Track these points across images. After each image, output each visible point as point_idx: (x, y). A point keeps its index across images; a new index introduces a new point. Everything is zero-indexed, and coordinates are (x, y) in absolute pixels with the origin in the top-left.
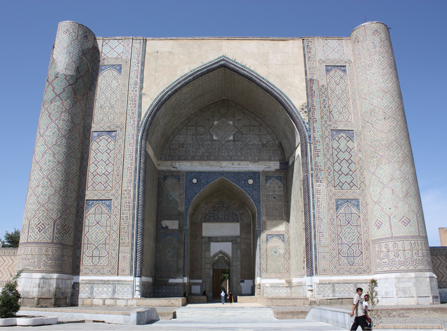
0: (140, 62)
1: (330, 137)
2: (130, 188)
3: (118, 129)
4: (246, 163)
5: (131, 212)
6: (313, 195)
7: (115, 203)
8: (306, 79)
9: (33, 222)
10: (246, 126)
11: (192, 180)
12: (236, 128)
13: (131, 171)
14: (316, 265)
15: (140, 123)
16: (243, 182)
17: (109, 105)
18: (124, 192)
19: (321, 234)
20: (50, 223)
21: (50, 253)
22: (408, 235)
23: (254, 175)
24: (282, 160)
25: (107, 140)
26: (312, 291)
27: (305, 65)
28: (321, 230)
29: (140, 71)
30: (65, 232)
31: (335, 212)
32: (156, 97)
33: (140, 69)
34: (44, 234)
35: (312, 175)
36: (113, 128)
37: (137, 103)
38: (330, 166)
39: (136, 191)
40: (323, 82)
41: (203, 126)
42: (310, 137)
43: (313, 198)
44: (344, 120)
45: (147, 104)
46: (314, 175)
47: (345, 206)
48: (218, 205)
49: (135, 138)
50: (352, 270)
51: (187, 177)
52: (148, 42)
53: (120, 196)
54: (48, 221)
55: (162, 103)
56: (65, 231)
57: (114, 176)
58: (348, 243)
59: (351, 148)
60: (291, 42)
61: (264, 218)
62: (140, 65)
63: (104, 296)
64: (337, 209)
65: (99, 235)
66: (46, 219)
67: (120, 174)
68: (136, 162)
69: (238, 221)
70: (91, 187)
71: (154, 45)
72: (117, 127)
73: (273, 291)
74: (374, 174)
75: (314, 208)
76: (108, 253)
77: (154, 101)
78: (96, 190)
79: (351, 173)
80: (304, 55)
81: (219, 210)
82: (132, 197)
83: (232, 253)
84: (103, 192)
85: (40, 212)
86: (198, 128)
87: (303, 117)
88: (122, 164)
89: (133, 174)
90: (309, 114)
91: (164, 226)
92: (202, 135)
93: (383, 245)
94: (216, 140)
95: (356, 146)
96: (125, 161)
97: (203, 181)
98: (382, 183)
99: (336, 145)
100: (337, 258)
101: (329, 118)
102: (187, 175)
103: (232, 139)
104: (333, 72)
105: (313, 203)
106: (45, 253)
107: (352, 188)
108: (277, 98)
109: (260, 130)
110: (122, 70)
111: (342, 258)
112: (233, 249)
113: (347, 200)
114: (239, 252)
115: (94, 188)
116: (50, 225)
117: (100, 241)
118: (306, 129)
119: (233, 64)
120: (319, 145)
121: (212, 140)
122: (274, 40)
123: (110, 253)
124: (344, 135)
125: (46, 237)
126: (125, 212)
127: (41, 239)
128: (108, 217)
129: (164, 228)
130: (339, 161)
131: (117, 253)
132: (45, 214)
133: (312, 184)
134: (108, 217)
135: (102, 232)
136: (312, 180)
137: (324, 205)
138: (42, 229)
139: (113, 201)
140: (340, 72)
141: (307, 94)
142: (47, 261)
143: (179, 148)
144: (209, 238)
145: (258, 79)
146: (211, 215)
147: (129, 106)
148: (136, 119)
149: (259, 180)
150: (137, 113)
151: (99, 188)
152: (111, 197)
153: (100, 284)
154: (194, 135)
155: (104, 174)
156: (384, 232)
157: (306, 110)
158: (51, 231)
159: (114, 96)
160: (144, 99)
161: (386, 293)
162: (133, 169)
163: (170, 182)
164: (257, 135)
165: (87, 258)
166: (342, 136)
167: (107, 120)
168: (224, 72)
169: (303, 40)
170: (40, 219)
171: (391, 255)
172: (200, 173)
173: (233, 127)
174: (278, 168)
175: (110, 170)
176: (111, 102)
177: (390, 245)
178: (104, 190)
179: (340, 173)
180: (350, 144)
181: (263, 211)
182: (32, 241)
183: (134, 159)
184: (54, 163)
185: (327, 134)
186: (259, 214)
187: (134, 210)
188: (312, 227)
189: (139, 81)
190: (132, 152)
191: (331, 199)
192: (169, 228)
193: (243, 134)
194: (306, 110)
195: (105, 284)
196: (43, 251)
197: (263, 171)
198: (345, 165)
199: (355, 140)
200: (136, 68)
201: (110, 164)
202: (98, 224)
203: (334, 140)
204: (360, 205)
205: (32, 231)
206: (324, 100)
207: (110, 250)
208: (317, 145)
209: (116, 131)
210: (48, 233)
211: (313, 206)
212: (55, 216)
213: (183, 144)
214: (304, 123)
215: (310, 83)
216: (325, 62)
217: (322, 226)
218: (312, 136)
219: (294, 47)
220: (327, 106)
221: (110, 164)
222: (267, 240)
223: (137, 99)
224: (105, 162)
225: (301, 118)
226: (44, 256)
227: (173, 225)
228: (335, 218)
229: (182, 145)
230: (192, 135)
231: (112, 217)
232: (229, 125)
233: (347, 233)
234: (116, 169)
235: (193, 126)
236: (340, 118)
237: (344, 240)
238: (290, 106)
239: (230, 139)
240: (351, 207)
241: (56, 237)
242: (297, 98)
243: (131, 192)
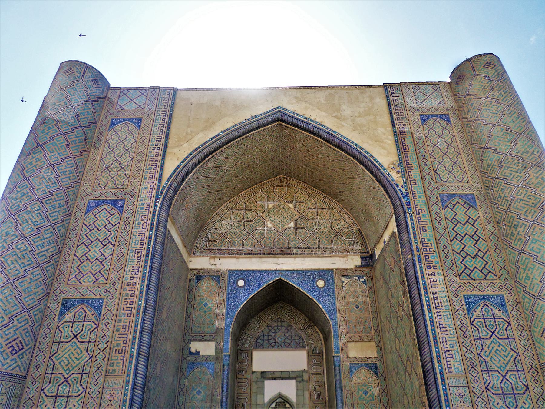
3: (127, 198)
6: (425, 289)
10: (311, 209)
11: (237, 282)
12: (298, 212)
13: (139, 255)
17: (118, 165)
18: (126, 286)
19: (447, 353)
23: (325, 274)
24: (364, 253)
25: (109, 212)
28: (448, 346)
30: (11, 352)
31: (467, 316)
35: (419, 258)
38: (446, 244)
39: (145, 284)
41: (253, 210)
42: (408, 204)
44: (456, 181)
46: (423, 258)
47: (482, 305)
48: (275, 324)
51: (229, 278)
56: (11, 349)
58: (499, 370)
59: (475, 219)
64: (469, 310)
65: (73, 358)
68: (149, 242)
69: (304, 347)
70: (74, 279)
75: (429, 309)
76: (85, 390)
78: (81, 284)
79: (481, 254)
81: (277, 331)
82: (137, 293)
83: (297, 396)
84: (91, 288)
87: (395, 179)
89: (143, 259)
91: (193, 350)
92: (252, 221)
95: (481, 216)
97: (253, 284)
100: (484, 397)
101: (434, 179)
103: (293, 226)
105: (428, 301)
107: (487, 278)
109: (330, 214)
111: (494, 396)
112: (297, 390)
114: (307, 394)
115: (78, 280)
117: (73, 368)
118: (402, 194)
119: (293, 117)
120: (424, 216)
121: (266, 228)
123: (88, 390)
124: (460, 201)
126: (123, 318)
128: (95, 326)
129: (193, 354)
130: (459, 238)
131: (100, 390)
133: (422, 272)
135: (79, 352)
137: (446, 304)
140: (441, 122)
143: (219, 238)
144: (263, 373)
146: (266, 338)
151: (85, 280)
152: (103, 295)
155: (97, 259)
157: (398, 169)
159: (128, 155)
163: (205, 284)
165: (46, 399)
166: (457, 202)
167: (113, 185)
173: (294, 212)
174: (360, 264)
175: (107, 252)
176: (122, 162)
178: (94, 283)
179: (464, 254)
180: (472, 213)
183: (147, 238)
185: (434, 199)
188: (432, 341)
189: (163, 137)
190: (144, 227)
192: (201, 354)
193: (306, 219)
199: (479, 207)
201: (110, 244)
202: (75, 340)
203: (446, 207)
204: (507, 305)
207: (89, 385)
208: (421, 216)
214: (398, 186)
215: (399, 137)
217: (448, 340)
220: (429, 163)
221: (110, 244)
224: (101, 242)
225: (393, 180)
227: (206, 349)
228: (469, 325)
229: (225, 235)
231: (100, 326)
232: (289, 208)
233: (493, 351)
235: (241, 210)
236: (450, 179)
237: (490, 363)
239: (290, 226)
240: (491, 307)
242: (385, 155)
243: (136, 287)
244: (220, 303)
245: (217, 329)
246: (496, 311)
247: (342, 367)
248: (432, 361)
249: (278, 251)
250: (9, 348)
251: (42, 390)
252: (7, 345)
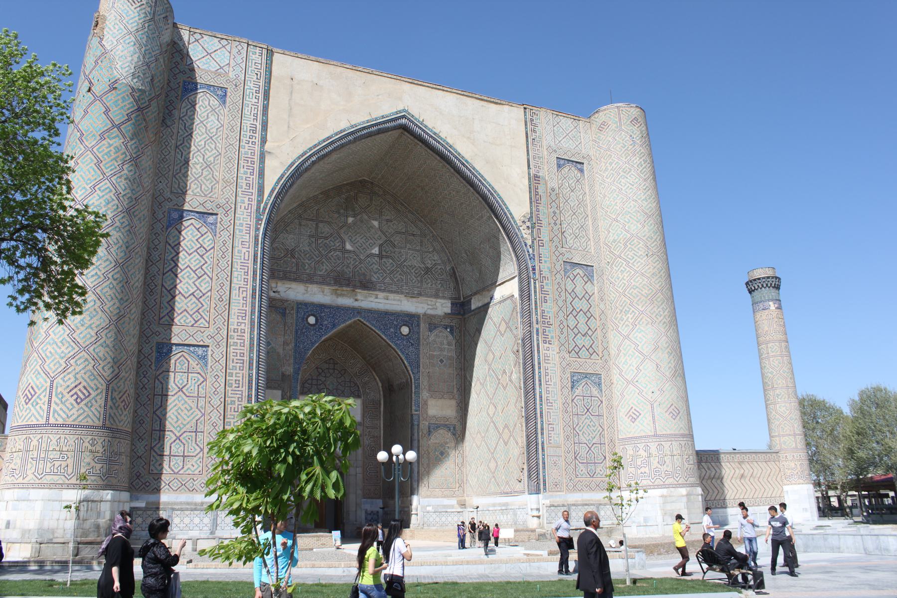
0: (262, 91)
1: (563, 273)
2: (243, 326)
3: (220, 211)
4: (397, 296)
5: (246, 372)
6: (539, 363)
7: (215, 353)
8: (529, 174)
9: (61, 382)
10: (399, 233)
12: (384, 234)
13: (245, 295)
14: (544, 476)
15: (262, 205)
16: (392, 330)
17: (201, 160)
20: (99, 385)
21: (99, 448)
22: (677, 432)
23: (411, 319)
24: (455, 299)
25: (198, 230)
26: (539, 517)
27: (528, 151)
29: (260, 108)
32: (290, 162)
33: (260, 104)
34: (86, 409)
35: (537, 331)
36: (209, 207)
37: (256, 166)
39: (256, 333)
40: (553, 184)
41: (328, 223)
42: (534, 269)
43: (539, 368)
45: (275, 171)
48: (326, 366)
49: (253, 233)
50: (593, 485)
52: (276, 57)
53: (225, 340)
54: (95, 381)
55: (298, 173)
57: (213, 301)
60: (506, 108)
61: (425, 394)
62: (261, 95)
63: (195, 534)
65: (182, 414)
66: (92, 378)
67: (226, 298)
68: (254, 280)
70: (167, 317)
71: (285, 64)
72: (219, 206)
73: (438, 519)
74: (627, 337)
75: (540, 384)
77: (288, 169)
79: (590, 332)
80: (527, 134)
81: (328, 375)
82: (247, 343)
84: (192, 331)
85: (78, 363)
86: (321, 225)
87: (525, 236)
88: (229, 279)
89: (249, 300)
90: (532, 232)
93: (641, 446)
94: (350, 252)
96: (235, 274)
97: (326, 322)
98: (641, 353)
99: (570, 287)
100: (573, 466)
102: (298, 308)
103: (377, 253)
104: (566, 169)
105: (540, 377)
106: (90, 447)
108: (484, 198)
110: (228, 100)
113: (586, 376)
116: (99, 391)
117: (185, 425)
119: (420, 128)
120: (547, 284)
121: (344, 250)
122: (482, 100)
124: (581, 272)
125: (90, 413)
126: (234, 372)
127: (81, 417)
128: (202, 379)
130: (574, 313)
132: (90, 367)
133: (538, 345)
134: (202, 379)
135: (189, 408)
136: (538, 340)
138: (83, 397)
139: (210, 349)
140: (576, 172)
141: (531, 199)
142: (93, 464)
143: (285, 256)
145: (460, 161)
146: (314, 382)
147: (242, 170)
148: (255, 197)
149: (419, 329)
150: (256, 186)
151: (182, 321)
153: (187, 510)
154: (313, 236)
155: (193, 294)
156: (643, 426)
157: (528, 224)
158: (102, 402)
159: (213, 146)
160: (268, 162)
161: (646, 519)
162: (250, 292)
164: (418, 251)
167: (199, 189)
168: (402, 137)
169: (525, 108)
170: (78, 376)
171: (654, 462)
172: (322, 307)
174: (448, 310)
175: (204, 288)
176: (206, 157)
177: (653, 447)
179: (576, 331)
180: (588, 286)
181: (424, 382)
182: (61, 421)
183: (251, 273)
184: (108, 263)
186: (418, 387)
187: (250, 369)
188: (539, 415)
189: (259, 127)
191: (564, 372)
193: (394, 246)
194: (528, 224)
195: (195, 509)
196: (86, 444)
197: (425, 314)
198: (582, 318)
200: (253, 101)
202: (181, 393)
205: (58, 401)
206: (555, 213)
209: (217, 214)
210: (96, 405)
211: (540, 381)
212: (109, 372)
213: (293, 250)
215: (534, 180)
216: (555, 151)
218: (537, 268)
219: (510, 117)
220: (558, 222)
222: (429, 432)
223: (256, 158)
224: (194, 272)
226: (88, 454)
230: (310, 236)
232: (373, 227)
234: (216, 287)
235: (312, 220)
237: (581, 437)
238: (505, 213)
239: (373, 251)
241: (110, 415)
242: (516, 204)
243: (246, 335)
244: (285, 343)
245: (283, 375)
246: (593, 389)
247: (421, 426)
248: (536, 433)
249: (358, 284)
251: (152, 448)
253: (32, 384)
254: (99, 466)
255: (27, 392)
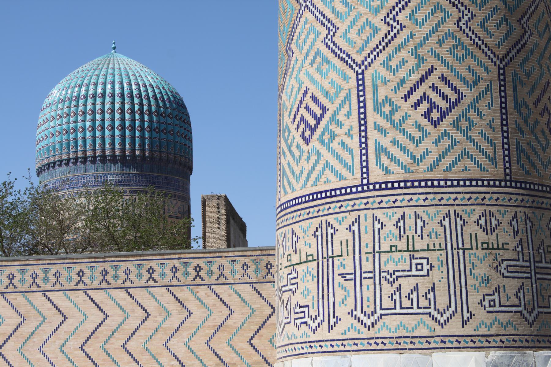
9: (383, 72)
20: (480, 71)
21: (505, 236)
34: (459, 137)
54: (469, 61)
66: (460, 53)
85: (419, 16)
106: (482, 236)
116: (482, 86)
125: (469, 146)
132: (450, 26)
138: (443, 105)
142: (497, 279)
158: (492, 114)
170: (424, 51)
182: (398, 174)
196: (472, 229)
205: (383, 123)
210: (481, 124)
212: (499, 35)
226: (481, 253)
241: (519, 149)
250: (416, 105)
252: (406, 98)
253: (313, 89)
254: (512, 285)
255: (303, 111)
